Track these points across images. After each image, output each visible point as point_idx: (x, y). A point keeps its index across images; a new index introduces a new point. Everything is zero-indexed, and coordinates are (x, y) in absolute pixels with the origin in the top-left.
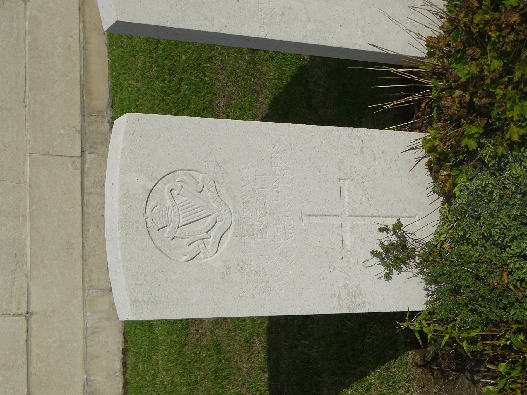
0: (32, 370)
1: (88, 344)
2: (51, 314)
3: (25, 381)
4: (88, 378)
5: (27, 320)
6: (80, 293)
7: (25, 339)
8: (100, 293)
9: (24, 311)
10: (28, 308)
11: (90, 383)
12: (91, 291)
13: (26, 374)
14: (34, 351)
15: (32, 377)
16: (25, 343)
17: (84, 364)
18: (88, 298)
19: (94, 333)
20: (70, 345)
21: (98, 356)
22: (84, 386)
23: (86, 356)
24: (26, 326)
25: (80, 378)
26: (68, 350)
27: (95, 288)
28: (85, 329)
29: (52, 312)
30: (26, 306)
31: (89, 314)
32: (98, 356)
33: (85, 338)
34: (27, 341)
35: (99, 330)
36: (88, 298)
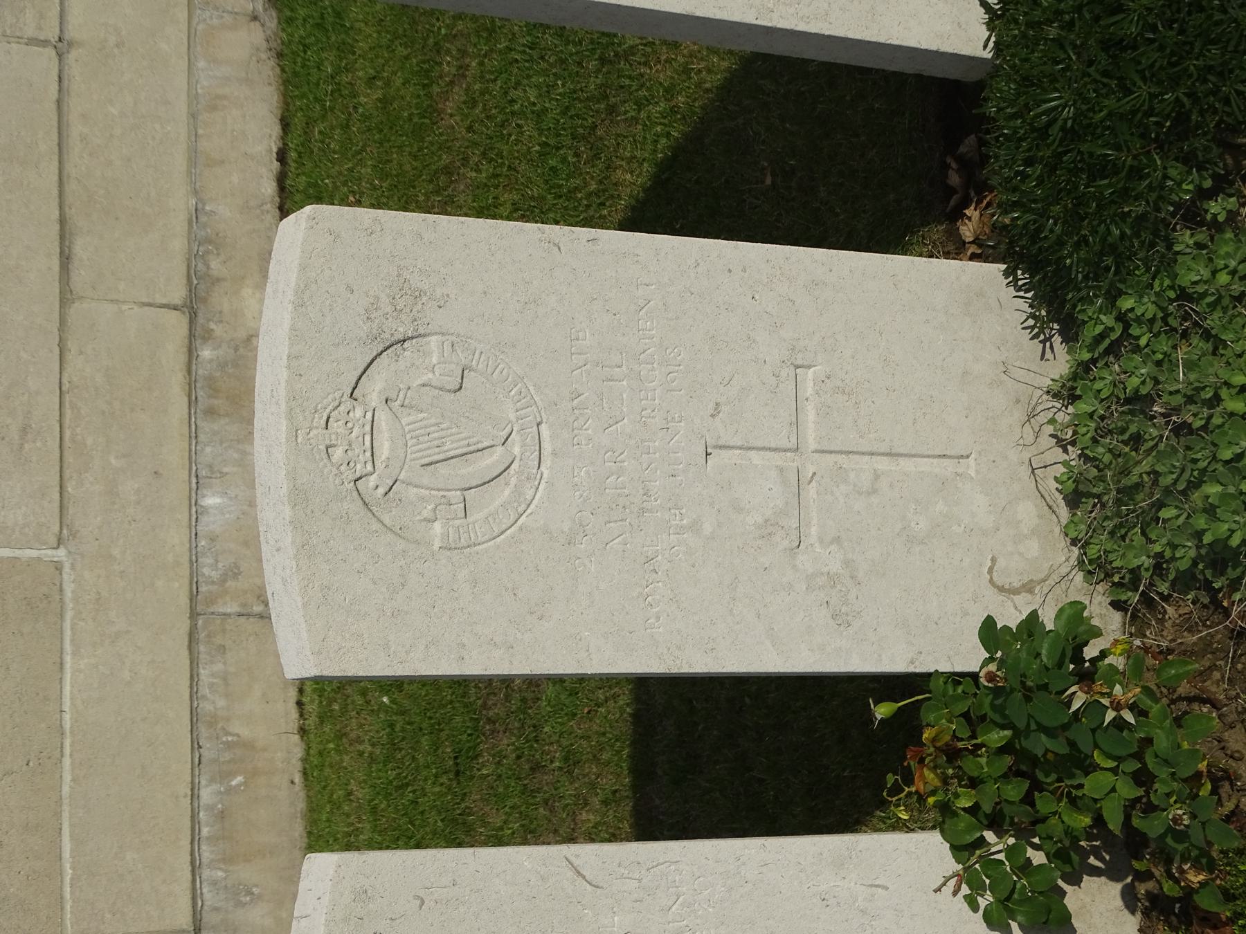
0: (70, 168)
1: (200, 132)
2: (116, 50)
3: (55, 192)
4: (200, 206)
5: (60, 55)
6: (183, 15)
7: (55, 96)
8: (228, 18)
9: (52, 34)
10: (61, 31)
11: (203, 219)
12: (208, 14)
13: (56, 178)
14: (76, 129)
15: (71, 187)
16: (54, 106)
17: (189, 173)
18: (200, 27)
19: (213, 108)
20: (157, 126)
21: (223, 162)
22: (190, 223)
23: (194, 157)
24: (56, 70)
25: (180, 203)
26: (154, 138)
27: (217, 8)
28: (193, 97)
29: (117, 46)
30: (57, 24)
31: (201, 64)
32: (223, 162)
33: (193, 116)
34: (59, 102)
35: (225, 103)
36: (200, 27)
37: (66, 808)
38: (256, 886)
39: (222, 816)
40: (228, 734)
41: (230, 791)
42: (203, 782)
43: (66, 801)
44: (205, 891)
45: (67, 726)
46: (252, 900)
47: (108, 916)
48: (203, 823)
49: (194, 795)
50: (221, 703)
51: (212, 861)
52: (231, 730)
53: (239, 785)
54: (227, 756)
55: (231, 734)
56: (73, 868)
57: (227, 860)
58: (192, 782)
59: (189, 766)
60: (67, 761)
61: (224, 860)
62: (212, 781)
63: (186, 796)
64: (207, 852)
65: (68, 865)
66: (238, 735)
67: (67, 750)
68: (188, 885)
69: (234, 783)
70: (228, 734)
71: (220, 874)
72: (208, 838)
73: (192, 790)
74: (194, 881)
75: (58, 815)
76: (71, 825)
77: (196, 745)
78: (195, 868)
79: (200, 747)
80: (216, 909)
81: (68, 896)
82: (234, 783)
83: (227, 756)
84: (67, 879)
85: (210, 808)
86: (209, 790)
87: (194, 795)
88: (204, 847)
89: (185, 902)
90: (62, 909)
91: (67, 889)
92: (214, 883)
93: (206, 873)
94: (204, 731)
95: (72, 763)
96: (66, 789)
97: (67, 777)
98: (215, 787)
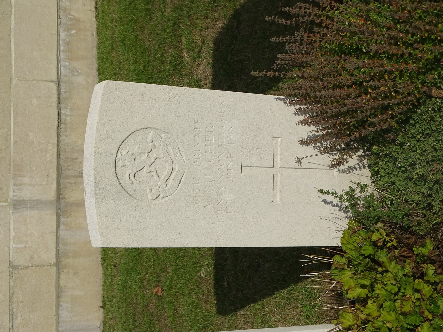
37: (12, 33)
38: (80, 69)
39: (68, 43)
40: (70, 15)
41: (71, 35)
42: (61, 31)
43: (12, 31)
44: (61, 69)
45: (13, 4)
46: (78, 74)
47: (27, 73)
48: (61, 45)
49: (58, 35)
50: (68, 4)
51: (64, 59)
52: (71, 13)
53: (74, 34)
54: (70, 23)
55: (71, 15)
56: (15, 54)
57: (70, 59)
58: (57, 30)
59: (56, 24)
60: (13, 17)
61: (69, 59)
62: (64, 30)
63: (55, 34)
64: (62, 56)
65: (13, 53)
66: (74, 16)
67: (13, 13)
68: (56, 65)
69: (72, 32)
70: (70, 15)
71: (67, 63)
72: (63, 51)
73: (57, 33)
74: (58, 65)
75: (9, 35)
76: (14, 39)
77: (59, 17)
78: (58, 60)
79: (60, 18)
80: (66, 76)
81: (13, 64)
82: (72, 32)
83: (70, 23)
84: (13, 58)
85: (64, 40)
86: (63, 34)
87: (58, 35)
88: (61, 54)
89: (54, 72)
90: (11, 68)
91: (13, 61)
92: (65, 67)
93: (62, 63)
94: (62, 13)
95: (15, 18)
96: (12, 27)
97: (13, 22)
98: (65, 33)
